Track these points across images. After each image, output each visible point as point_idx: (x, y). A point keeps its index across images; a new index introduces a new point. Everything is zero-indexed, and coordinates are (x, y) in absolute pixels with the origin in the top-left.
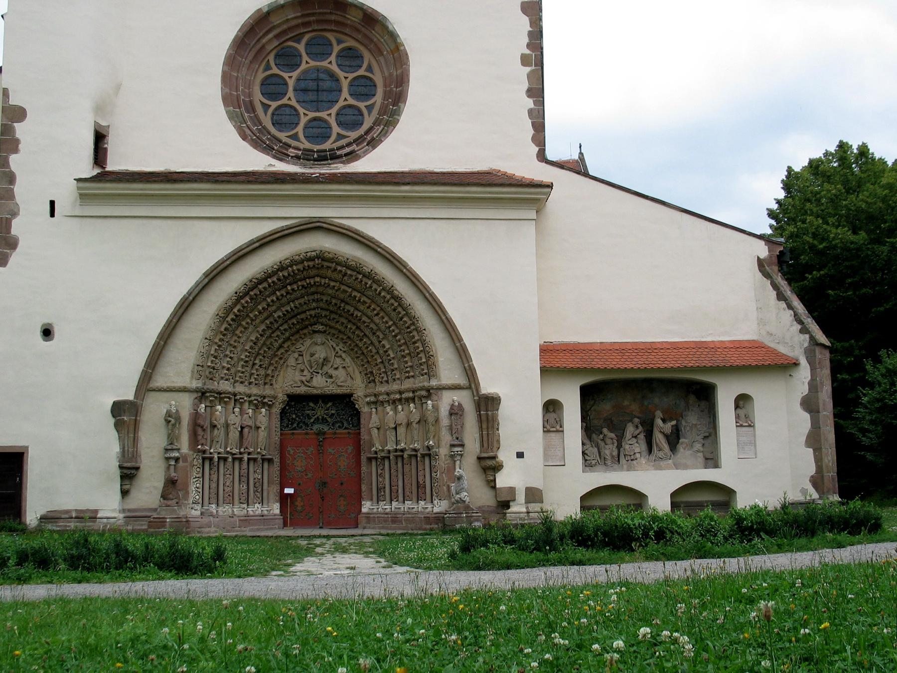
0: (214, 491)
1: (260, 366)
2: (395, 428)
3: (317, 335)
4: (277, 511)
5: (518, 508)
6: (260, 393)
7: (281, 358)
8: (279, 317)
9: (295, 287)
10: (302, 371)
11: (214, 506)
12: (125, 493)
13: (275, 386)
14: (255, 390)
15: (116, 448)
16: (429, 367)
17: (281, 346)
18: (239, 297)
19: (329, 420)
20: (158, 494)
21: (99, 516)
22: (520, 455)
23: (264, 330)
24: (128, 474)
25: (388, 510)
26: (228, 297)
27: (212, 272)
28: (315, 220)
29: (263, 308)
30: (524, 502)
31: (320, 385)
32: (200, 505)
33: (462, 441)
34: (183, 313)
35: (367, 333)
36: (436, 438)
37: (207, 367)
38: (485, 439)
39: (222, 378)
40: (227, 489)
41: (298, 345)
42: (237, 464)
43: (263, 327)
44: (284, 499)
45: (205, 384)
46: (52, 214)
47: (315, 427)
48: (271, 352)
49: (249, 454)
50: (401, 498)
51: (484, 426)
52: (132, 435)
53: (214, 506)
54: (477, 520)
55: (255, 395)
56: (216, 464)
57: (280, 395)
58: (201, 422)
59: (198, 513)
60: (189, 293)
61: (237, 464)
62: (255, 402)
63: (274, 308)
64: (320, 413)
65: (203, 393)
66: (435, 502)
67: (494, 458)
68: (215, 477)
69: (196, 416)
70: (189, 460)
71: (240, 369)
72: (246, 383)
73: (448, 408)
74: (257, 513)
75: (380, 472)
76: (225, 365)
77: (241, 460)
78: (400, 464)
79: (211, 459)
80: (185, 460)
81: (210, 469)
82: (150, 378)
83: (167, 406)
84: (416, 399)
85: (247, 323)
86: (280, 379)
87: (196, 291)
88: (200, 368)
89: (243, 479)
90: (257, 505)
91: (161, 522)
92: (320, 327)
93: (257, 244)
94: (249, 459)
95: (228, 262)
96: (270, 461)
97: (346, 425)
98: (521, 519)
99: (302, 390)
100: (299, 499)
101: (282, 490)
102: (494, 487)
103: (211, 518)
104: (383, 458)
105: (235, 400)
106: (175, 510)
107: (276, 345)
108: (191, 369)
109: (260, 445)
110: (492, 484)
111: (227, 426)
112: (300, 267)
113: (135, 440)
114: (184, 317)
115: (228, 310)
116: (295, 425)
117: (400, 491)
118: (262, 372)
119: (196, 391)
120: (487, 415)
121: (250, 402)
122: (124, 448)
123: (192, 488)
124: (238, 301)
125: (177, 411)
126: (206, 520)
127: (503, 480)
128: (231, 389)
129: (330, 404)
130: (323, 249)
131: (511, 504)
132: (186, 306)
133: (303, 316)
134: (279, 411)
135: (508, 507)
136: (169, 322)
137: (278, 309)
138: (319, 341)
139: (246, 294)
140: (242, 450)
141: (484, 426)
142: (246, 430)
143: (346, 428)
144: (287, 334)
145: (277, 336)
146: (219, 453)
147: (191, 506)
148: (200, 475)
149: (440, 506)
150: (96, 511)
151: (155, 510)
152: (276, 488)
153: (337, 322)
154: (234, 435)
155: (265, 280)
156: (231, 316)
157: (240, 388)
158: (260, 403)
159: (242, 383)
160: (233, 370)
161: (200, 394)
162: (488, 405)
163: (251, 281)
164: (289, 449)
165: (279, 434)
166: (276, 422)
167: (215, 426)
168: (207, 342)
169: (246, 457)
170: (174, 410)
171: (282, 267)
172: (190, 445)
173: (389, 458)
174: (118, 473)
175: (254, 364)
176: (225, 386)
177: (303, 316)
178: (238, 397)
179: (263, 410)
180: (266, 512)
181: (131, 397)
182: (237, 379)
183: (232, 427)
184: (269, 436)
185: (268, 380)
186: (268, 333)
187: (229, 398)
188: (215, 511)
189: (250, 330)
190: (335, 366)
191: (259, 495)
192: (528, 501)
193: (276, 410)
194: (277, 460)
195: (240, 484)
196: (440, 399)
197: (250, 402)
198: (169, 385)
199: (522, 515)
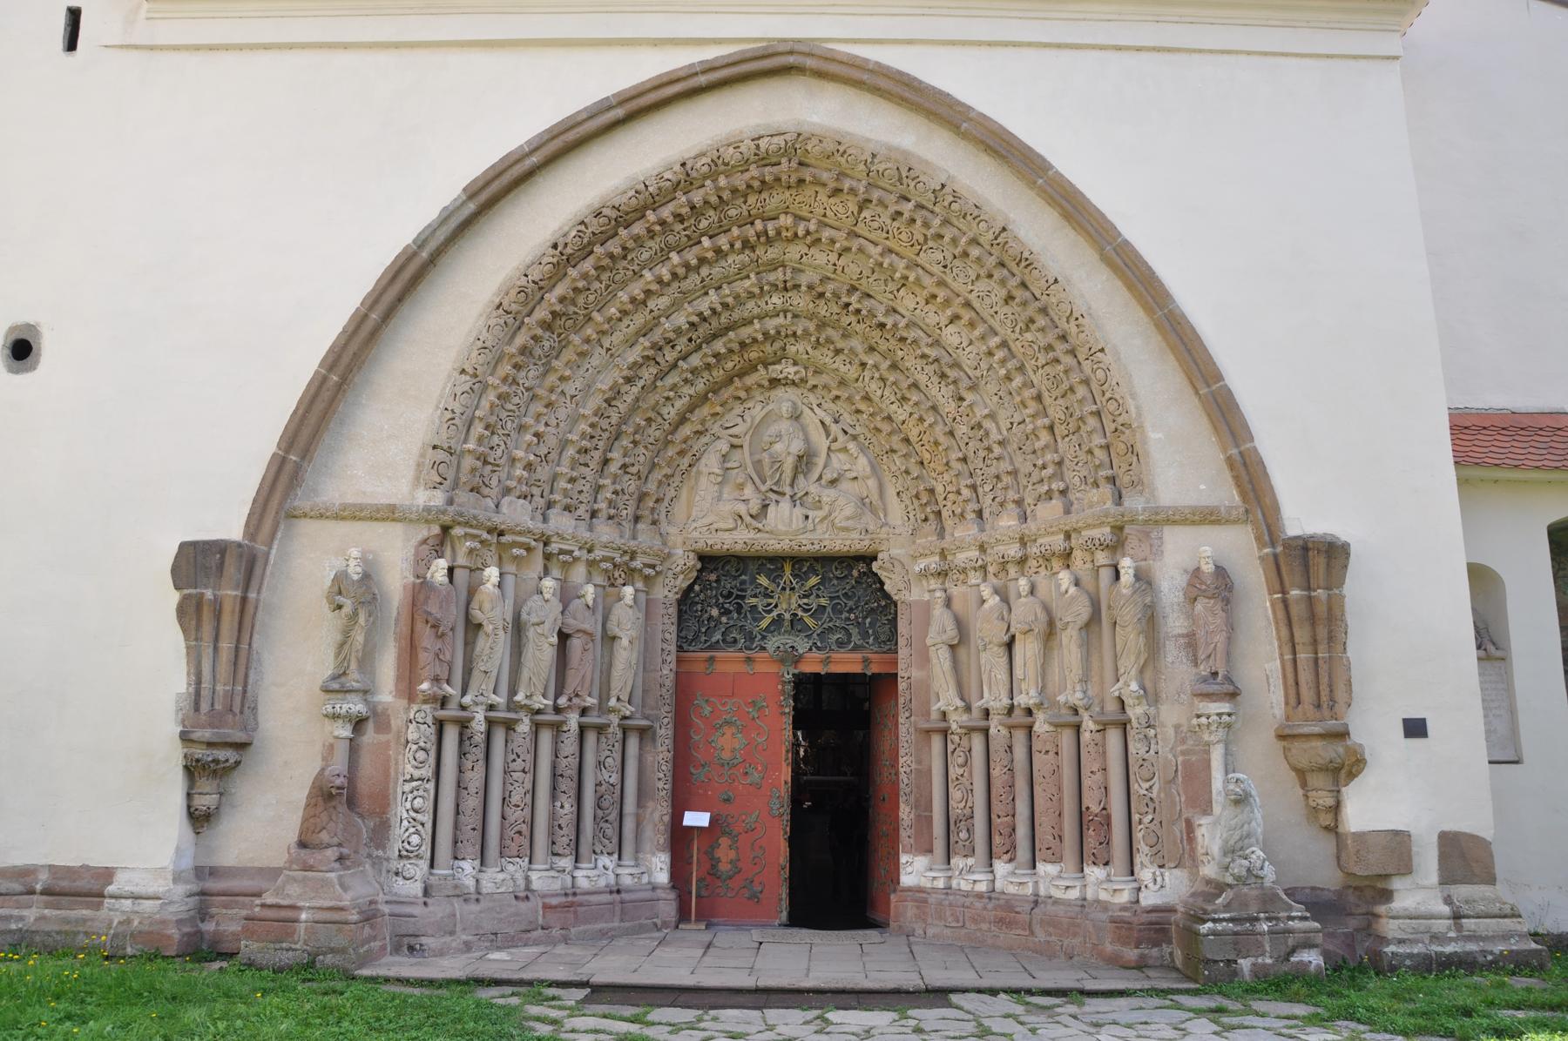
0: (471, 820)
1: (624, 466)
2: (1010, 645)
3: (779, 392)
4: (663, 877)
5: (1418, 898)
6: (619, 542)
7: (681, 453)
8: (678, 331)
9: (723, 242)
10: (741, 487)
11: (468, 866)
12: (199, 819)
14: (605, 532)
15: (178, 682)
16: (1119, 462)
17: (683, 420)
18: (565, 256)
19: (810, 622)
20: (290, 831)
21: (111, 889)
22: (1415, 728)
23: (635, 366)
24: (214, 761)
25: (982, 888)
26: (528, 260)
27: (488, 184)
28: (781, 48)
29: (633, 300)
30: (1434, 878)
31: (785, 528)
32: (424, 865)
33: (1228, 679)
34: (400, 299)
35: (922, 379)
36: (1148, 674)
37: (466, 460)
38: (1305, 676)
39: (507, 491)
40: (515, 815)
41: (731, 419)
42: (546, 737)
43: (633, 355)
44: (679, 838)
45: (450, 502)
46: (71, 45)
47: (773, 643)
48: (654, 433)
49: (584, 711)
50: (1023, 853)
51: (1302, 635)
52: (226, 645)
53: (468, 866)
54: (1308, 945)
56: (479, 738)
57: (680, 552)
58: (434, 609)
59: (416, 888)
60: (421, 242)
61: (546, 737)
62: (608, 565)
63: (663, 302)
64: (788, 603)
65: (446, 529)
66: (1146, 874)
67: (1343, 735)
68: (475, 779)
69: (421, 589)
70: (396, 723)
71: (564, 469)
72: (581, 511)
73: (1181, 580)
74: (602, 883)
75: (954, 772)
76: (520, 454)
77: (557, 728)
78: (1020, 752)
79: (464, 725)
80: (383, 725)
81: (462, 754)
82: (296, 479)
83: (339, 564)
84: (1077, 554)
85: (587, 341)
86: (679, 510)
87: (441, 235)
88: (441, 455)
89: (564, 785)
90: (605, 860)
91: (284, 919)
92: (789, 370)
93: (619, 113)
94: (582, 729)
95: (534, 160)
96: (643, 732)
97: (856, 638)
98: (1435, 938)
99: (738, 540)
100: (724, 841)
101: (677, 817)
102: (1333, 829)
103: (457, 904)
104: (971, 730)
105: (548, 557)
106: (326, 883)
107: (670, 412)
108: (416, 450)
109: (616, 685)
110: (1327, 819)
111: (518, 628)
112: (739, 181)
113: (242, 663)
114: (405, 309)
115: (531, 292)
116: (718, 636)
117: (1022, 831)
118: (631, 485)
119: (426, 515)
120: (1310, 601)
121: (592, 564)
122: (199, 682)
123: (401, 810)
124: (558, 270)
125: (366, 577)
126: (438, 909)
127: (1367, 809)
128: (537, 526)
129: (814, 580)
130: (805, 129)
131: (1397, 884)
132: (410, 277)
133: (745, 333)
134: (673, 597)
135: (1387, 896)
136: (359, 320)
137: (676, 305)
138: (785, 408)
139: (586, 251)
140: (562, 701)
141: (1302, 635)
142: (576, 643)
143: (856, 648)
144: (700, 386)
145: (673, 387)
146: (491, 707)
147: (396, 865)
148: (427, 772)
149: (1163, 887)
150: (108, 874)
151: (274, 873)
152: (659, 811)
153: (838, 352)
154: (541, 652)
155: (640, 213)
156: (541, 313)
157: (560, 522)
158: (620, 570)
159: (567, 508)
160: (543, 473)
161: (436, 530)
162: (1311, 571)
163: (598, 215)
165: (672, 658)
166: (667, 626)
167: (480, 626)
168: (465, 382)
169: (573, 720)
170: (355, 571)
171: (686, 179)
172: (399, 678)
173: (986, 731)
174: (174, 757)
175: (606, 462)
176: (516, 513)
177: (745, 333)
178: (554, 547)
179: (628, 591)
180: (627, 881)
181: (230, 526)
182: (556, 497)
183: (531, 633)
184: (645, 664)
185: (645, 509)
186: (648, 373)
187: (529, 549)
188: (470, 883)
189: (595, 361)
190: (828, 476)
191: (610, 831)
192: (1447, 878)
193: (667, 592)
194: (665, 733)
195: (554, 797)
196: (1157, 552)
198: (351, 499)
199: (1441, 925)
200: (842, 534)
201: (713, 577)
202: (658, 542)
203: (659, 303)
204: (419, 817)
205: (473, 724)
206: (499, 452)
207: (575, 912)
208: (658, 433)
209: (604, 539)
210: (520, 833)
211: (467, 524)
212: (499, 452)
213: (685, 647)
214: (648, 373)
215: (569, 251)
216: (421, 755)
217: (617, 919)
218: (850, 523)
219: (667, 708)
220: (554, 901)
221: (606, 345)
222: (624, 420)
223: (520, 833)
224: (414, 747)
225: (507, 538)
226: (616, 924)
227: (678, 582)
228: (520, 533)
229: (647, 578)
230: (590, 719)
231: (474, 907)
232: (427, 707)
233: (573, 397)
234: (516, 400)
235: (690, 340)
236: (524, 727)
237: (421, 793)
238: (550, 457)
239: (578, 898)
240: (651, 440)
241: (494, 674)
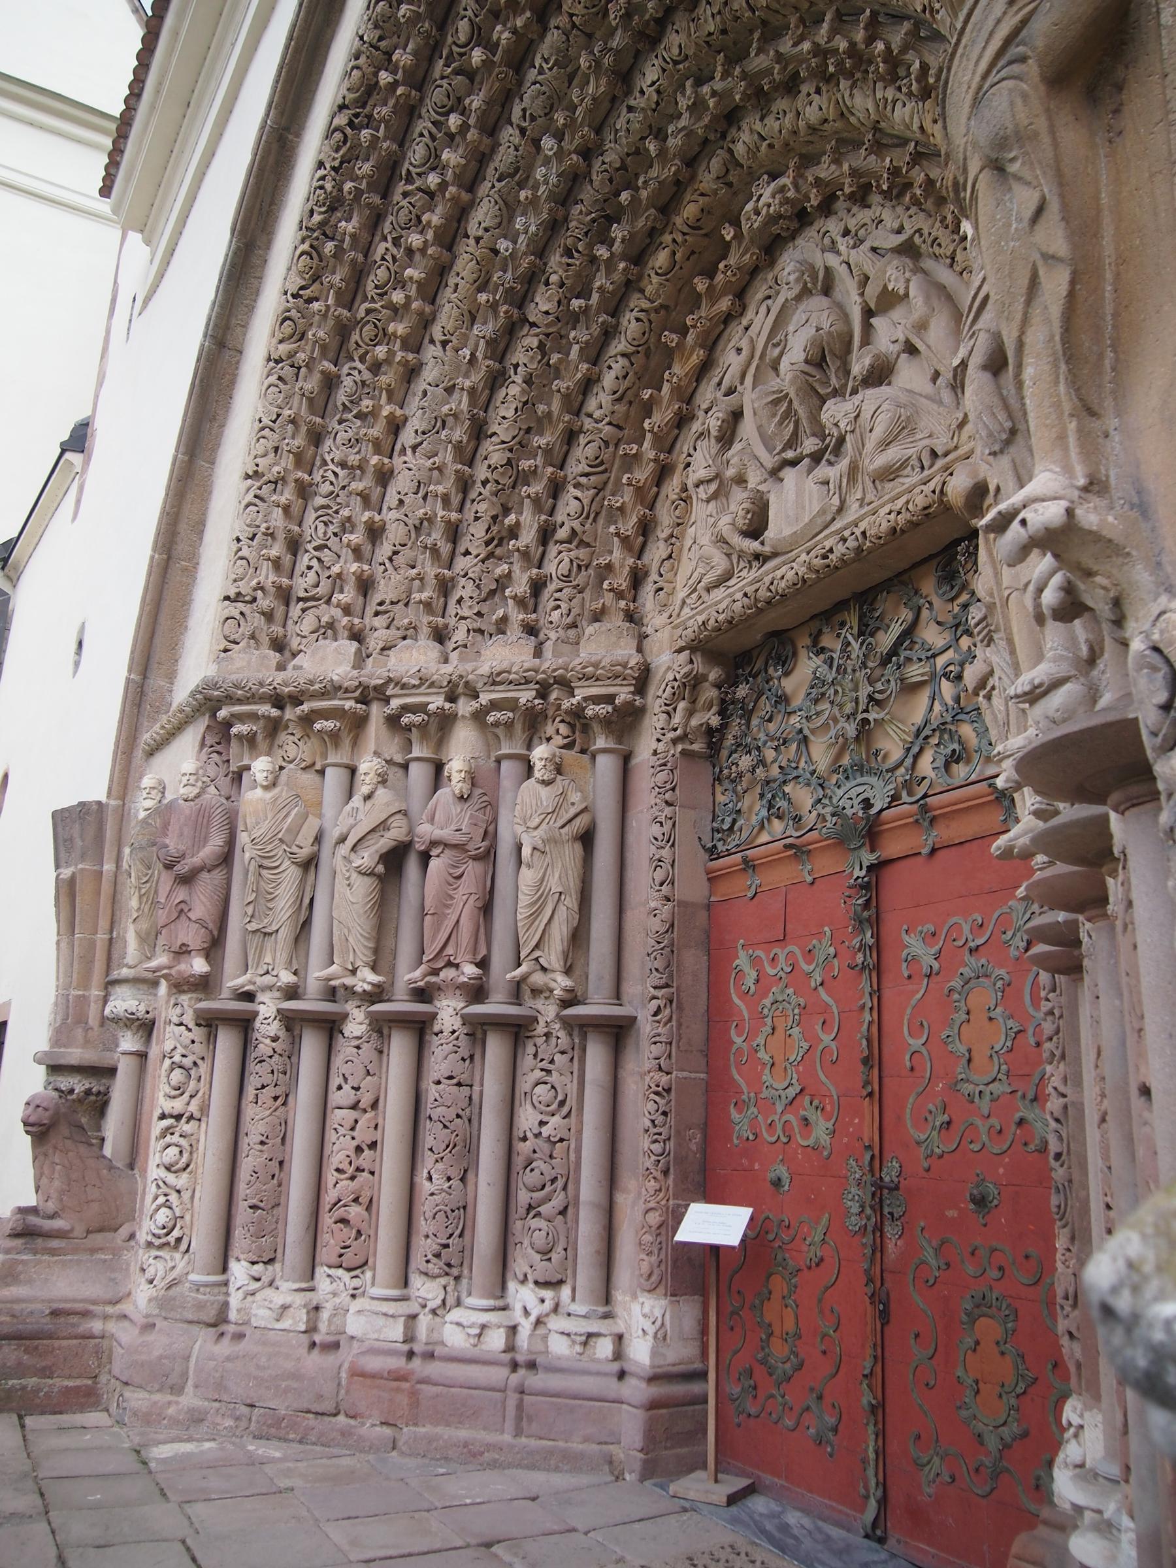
4: (640, 1352)
13: (654, 620)
40: (336, 1188)
42: (400, 1046)
44: (694, 1272)
49: (477, 992)
55: (494, 681)
77: (420, 1028)
79: (244, 1024)
89: (433, 1136)
94: (477, 1030)
96: (618, 1032)
121: (479, 716)
160: (386, 590)
164: (742, 960)
176: (328, 662)
180: (559, 1347)
197: (479, 716)
200: (891, 488)
201: (742, 691)
202: (626, 652)
203: (483, 215)
204: (171, 1178)
205: (257, 1024)
206: (311, 575)
207: (414, 1394)
208: (590, 451)
209: (485, 669)
210: (344, 1221)
211: (230, 699)
212: (311, 575)
213: (721, 847)
214: (523, 354)
215: (317, 218)
216: (177, 1076)
217: (509, 1424)
218: (893, 454)
219: (655, 978)
220: (375, 1364)
221: (438, 336)
222: (520, 447)
223: (344, 1221)
224: (167, 1062)
225: (305, 707)
226: (507, 1438)
227: (677, 720)
228: (323, 694)
229: (607, 723)
230: (494, 1007)
231: (225, 1348)
232: (185, 999)
233: (414, 448)
234: (326, 488)
235: (568, 253)
236: (356, 1025)
237: (175, 1139)
238: (400, 560)
239: (434, 1369)
240: (583, 467)
241: (285, 935)
